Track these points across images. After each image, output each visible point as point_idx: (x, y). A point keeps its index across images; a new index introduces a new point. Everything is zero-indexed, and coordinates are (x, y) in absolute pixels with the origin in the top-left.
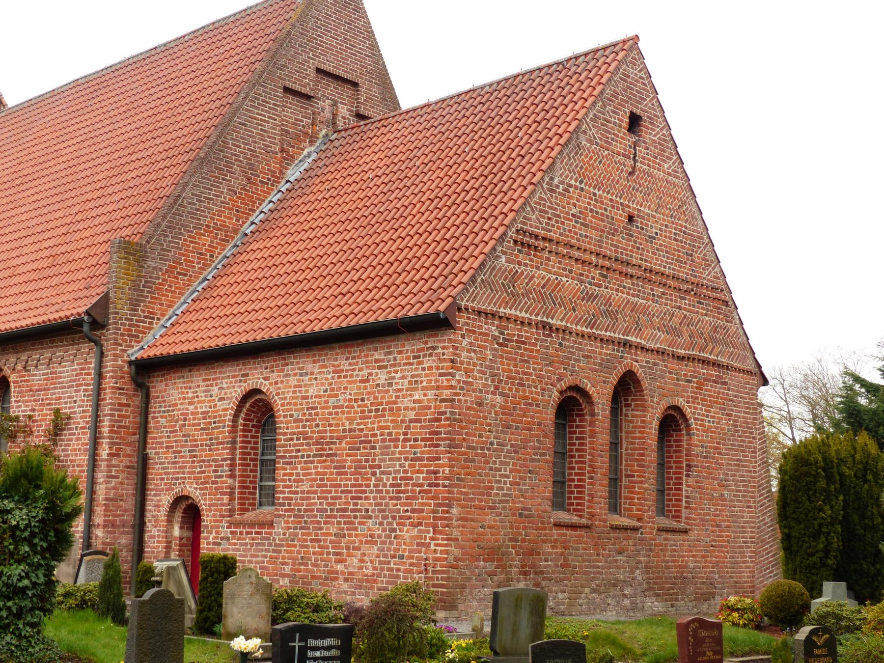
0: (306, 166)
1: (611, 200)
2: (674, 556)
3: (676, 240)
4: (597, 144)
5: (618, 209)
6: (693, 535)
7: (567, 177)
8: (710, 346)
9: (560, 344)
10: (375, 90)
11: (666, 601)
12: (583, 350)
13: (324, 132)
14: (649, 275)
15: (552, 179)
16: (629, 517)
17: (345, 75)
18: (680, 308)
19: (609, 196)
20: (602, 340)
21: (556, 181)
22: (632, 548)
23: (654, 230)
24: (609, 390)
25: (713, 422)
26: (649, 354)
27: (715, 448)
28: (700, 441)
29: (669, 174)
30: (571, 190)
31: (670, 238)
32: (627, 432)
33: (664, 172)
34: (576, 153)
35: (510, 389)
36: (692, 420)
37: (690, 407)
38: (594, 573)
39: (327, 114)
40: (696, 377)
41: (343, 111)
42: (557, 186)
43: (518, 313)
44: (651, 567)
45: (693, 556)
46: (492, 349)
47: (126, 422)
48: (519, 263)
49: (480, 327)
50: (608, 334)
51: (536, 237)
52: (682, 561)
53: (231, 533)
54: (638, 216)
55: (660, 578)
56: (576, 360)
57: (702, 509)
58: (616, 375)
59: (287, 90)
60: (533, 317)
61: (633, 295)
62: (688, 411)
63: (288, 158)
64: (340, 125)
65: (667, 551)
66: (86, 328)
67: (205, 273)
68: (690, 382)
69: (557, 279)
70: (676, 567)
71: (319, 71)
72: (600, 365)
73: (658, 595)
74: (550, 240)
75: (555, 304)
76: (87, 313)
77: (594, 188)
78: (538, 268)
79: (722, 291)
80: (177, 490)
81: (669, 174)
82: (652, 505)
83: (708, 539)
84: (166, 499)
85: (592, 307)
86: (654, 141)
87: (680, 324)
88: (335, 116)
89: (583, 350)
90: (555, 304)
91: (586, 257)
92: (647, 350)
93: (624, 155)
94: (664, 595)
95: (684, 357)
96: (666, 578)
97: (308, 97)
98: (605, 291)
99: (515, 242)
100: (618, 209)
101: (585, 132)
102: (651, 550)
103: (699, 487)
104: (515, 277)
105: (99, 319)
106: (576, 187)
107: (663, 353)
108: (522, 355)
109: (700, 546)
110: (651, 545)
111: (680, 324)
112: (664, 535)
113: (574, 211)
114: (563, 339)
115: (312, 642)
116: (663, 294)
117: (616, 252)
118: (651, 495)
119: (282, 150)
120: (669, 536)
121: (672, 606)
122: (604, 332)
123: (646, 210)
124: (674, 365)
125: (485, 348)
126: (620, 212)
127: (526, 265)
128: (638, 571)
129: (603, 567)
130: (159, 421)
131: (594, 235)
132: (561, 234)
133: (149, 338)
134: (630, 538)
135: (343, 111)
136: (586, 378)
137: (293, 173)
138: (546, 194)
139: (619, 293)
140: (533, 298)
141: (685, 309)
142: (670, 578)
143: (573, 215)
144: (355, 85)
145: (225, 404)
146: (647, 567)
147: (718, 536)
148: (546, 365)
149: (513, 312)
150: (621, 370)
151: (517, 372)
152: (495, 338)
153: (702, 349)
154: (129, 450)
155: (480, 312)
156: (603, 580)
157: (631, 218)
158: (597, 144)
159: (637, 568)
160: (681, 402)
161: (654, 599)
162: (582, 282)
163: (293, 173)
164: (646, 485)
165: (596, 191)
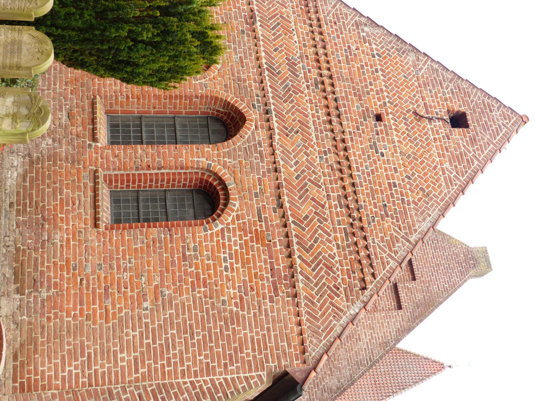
2: (68, 205)
3: (389, 184)
6: (92, 235)
7: (374, 39)
11: (18, 193)
14: (341, 146)
15: (366, 25)
19: (384, 88)
21: (366, 29)
22: (74, 131)
23: (384, 151)
25: (226, 268)
26: (268, 141)
28: (200, 242)
30: (367, 44)
36: (220, 226)
37: (233, 222)
38: (49, 79)
40: (267, 230)
44: (55, 164)
45: (68, 240)
50: (267, 78)
52: (62, 219)
54: (385, 125)
55: (43, 183)
56: (235, 49)
57: (124, 258)
58: (236, 102)
61: (314, 122)
65: (73, 192)
69: (293, 30)
70: (55, 207)
72: (240, 80)
73: (24, 180)
75: (273, 29)
79: (373, 275)
82: (120, 160)
83: (89, 270)
85: (285, 69)
87: (313, 199)
90: (273, 29)
92: (271, 145)
93: (425, 104)
94: (25, 187)
95: (281, 206)
96: (44, 189)
98: (304, 85)
102: (73, 162)
107: (276, 170)
109: (81, 255)
110: (79, 164)
111: (313, 199)
112: (90, 184)
113: (353, 48)
118: (130, 159)
120: (90, 193)
121: (11, 205)
122: (269, 84)
123: (396, 139)
124: (270, 191)
126: (379, 103)
128: (50, 142)
129: (55, 89)
131: (345, 71)
134: (84, 129)
136: (224, 62)
138: (352, 19)
139: (309, 101)
140: (270, 8)
141: (330, 207)
142: (43, 200)
143: (349, 47)
146: (55, 154)
147: (94, 292)
148: (222, 18)
156: (43, 90)
157: (379, 118)
159: (54, 140)
160: (235, 204)
161: (20, 170)
162: (301, 57)
164: (140, 151)
165: (380, 73)
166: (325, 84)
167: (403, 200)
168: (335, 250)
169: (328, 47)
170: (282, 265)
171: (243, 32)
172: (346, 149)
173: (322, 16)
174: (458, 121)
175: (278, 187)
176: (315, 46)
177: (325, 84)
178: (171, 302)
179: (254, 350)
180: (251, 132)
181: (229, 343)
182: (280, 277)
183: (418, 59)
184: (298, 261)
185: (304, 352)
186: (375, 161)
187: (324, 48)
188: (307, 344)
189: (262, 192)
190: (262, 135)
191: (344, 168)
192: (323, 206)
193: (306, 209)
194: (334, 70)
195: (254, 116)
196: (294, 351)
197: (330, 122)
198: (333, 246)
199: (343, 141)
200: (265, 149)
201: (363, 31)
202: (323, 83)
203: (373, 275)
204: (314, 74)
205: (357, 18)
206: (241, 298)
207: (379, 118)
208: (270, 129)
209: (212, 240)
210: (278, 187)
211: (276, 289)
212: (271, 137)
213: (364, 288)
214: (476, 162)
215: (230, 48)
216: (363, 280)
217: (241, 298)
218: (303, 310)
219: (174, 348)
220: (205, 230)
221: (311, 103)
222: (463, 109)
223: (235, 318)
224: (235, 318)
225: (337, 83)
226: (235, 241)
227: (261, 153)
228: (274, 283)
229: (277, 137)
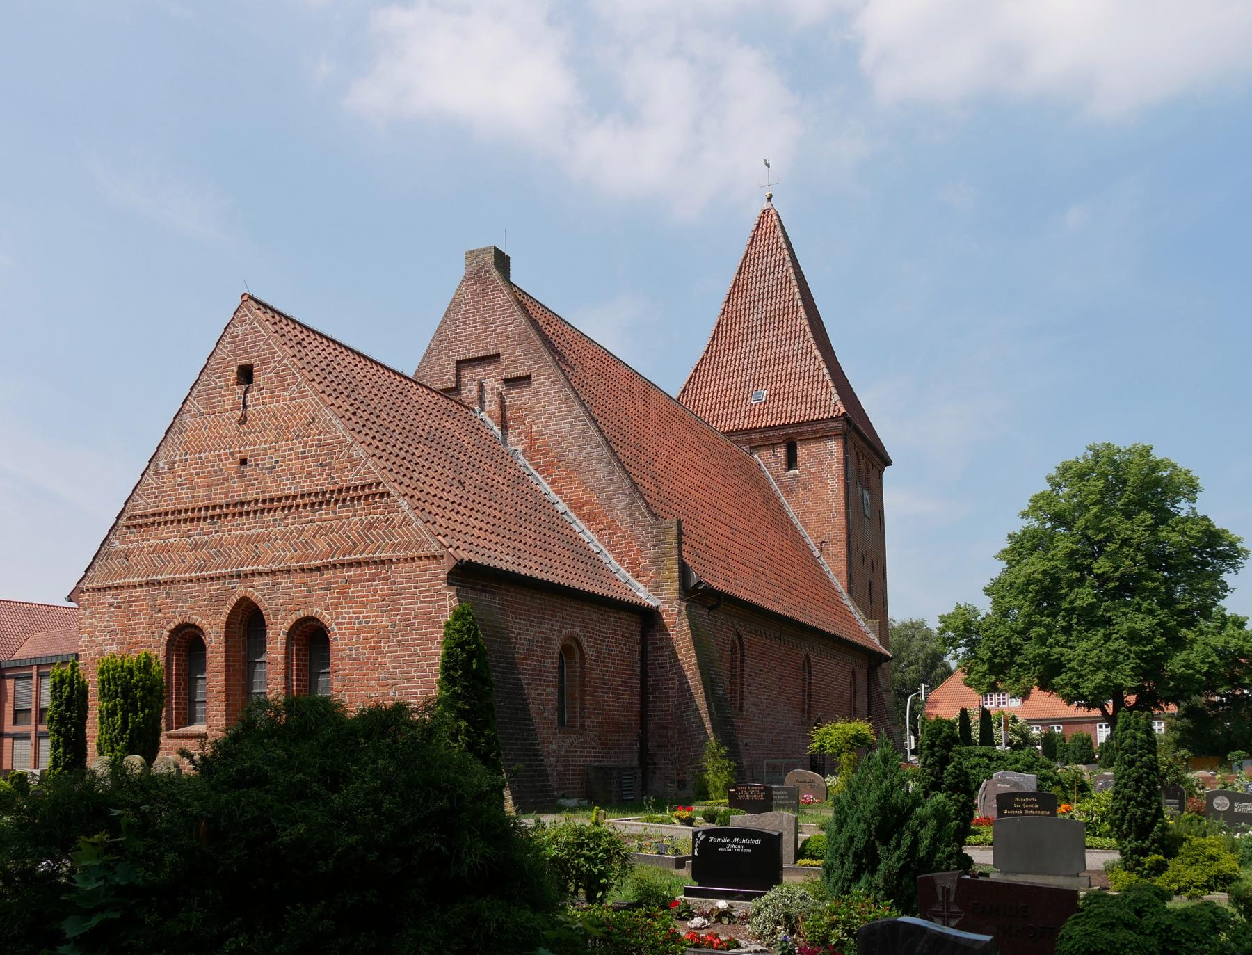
5: (227, 459)
14: (268, 504)
21: (161, 465)
24: (223, 618)
25: (367, 622)
27: (374, 648)
37: (330, 614)
48: (131, 542)
74: (160, 514)
79: (379, 484)
81: (294, 399)
85: (202, 554)
92: (267, 574)
95: (318, 569)
99: (128, 527)
101: (189, 411)
103: (347, 690)
107: (288, 571)
117: (226, 497)
123: (263, 446)
124: (306, 578)
131: (201, 492)
141: (320, 520)
155: (99, 590)
157: (244, 462)
158: (202, 414)
160: (314, 611)
166: (216, 513)
167: (318, 446)
168: (357, 519)
169: (179, 507)
170: (366, 571)
171: (167, 594)
172: (272, 500)
173: (150, 511)
174: (246, 375)
175: (303, 570)
176: (179, 521)
177: (216, 513)
178: (390, 673)
179: (430, 602)
180: (255, 590)
181: (424, 623)
182: (376, 574)
183: (189, 411)
184: (364, 555)
185: (435, 557)
186: (283, 471)
187: (180, 512)
188: (428, 553)
189: (306, 585)
190: (258, 581)
191: (287, 503)
192: (321, 528)
193: (322, 544)
194: (200, 504)
195: (242, 589)
196: (433, 565)
197: (248, 513)
198: (353, 518)
199: (264, 502)
200: (270, 580)
202: (212, 517)
203: (379, 484)
204: (205, 525)
206: (391, 610)
207: (244, 462)
208: (253, 574)
209: (344, 634)
210: (303, 570)
211: (384, 578)
212: (260, 574)
213: (388, 494)
214: (285, 361)
216: (382, 495)
217: (391, 610)
218: (402, 554)
219: (424, 671)
220: (336, 639)
221: (230, 530)
222: (235, 368)
223: (405, 617)
224: (405, 617)
225: (212, 502)
226: (345, 612)
227: (274, 584)
228: (380, 580)
229: (260, 567)
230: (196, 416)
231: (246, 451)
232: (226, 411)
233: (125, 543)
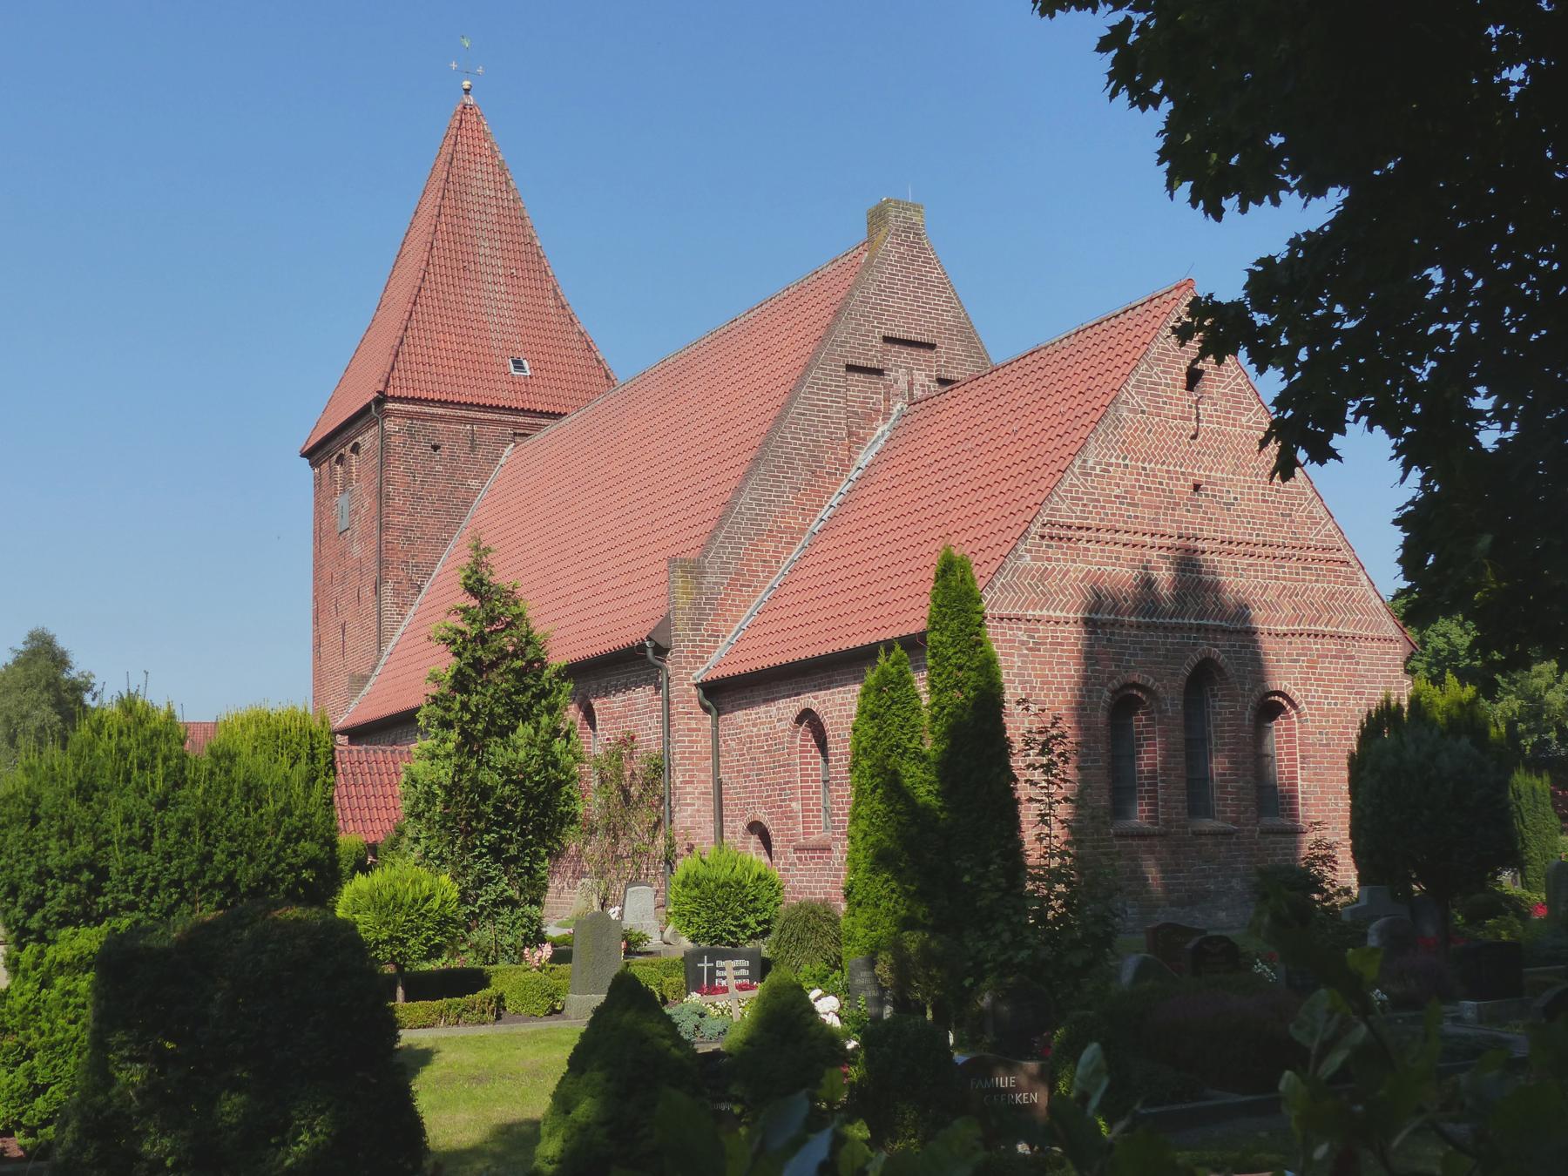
0: (877, 448)
1: (1168, 472)
4: (1143, 412)
5: (1178, 479)
8: (1326, 616)
9: (1109, 640)
10: (958, 348)
12: (1140, 643)
13: (898, 407)
15: (1085, 461)
16: (1224, 820)
17: (919, 338)
18: (1277, 578)
20: (1165, 628)
21: (1090, 463)
24: (1181, 681)
26: (1234, 637)
27: (1341, 734)
29: (1250, 428)
31: (1257, 501)
32: (1216, 726)
33: (1241, 426)
34: (1116, 427)
35: (1047, 696)
39: (903, 385)
41: (920, 377)
42: (1093, 468)
43: (1051, 613)
46: (1020, 656)
47: (698, 747)
48: (1049, 559)
49: (1004, 634)
51: (1069, 527)
53: (799, 859)
59: (851, 368)
60: (1071, 615)
62: (1296, 696)
63: (856, 439)
64: (918, 393)
66: (650, 653)
67: (772, 581)
68: (1297, 661)
71: (887, 339)
72: (1166, 656)
76: (649, 638)
77: (1144, 460)
78: (1074, 561)
80: (749, 817)
81: (1250, 428)
84: (742, 825)
86: (1224, 394)
88: (911, 385)
89: (1140, 643)
91: (1138, 538)
92: (1231, 633)
97: (879, 372)
99: (1043, 537)
100: (1178, 479)
104: (1045, 575)
105: (663, 643)
106: (1118, 465)
108: (1060, 657)
112: (1272, 838)
113: (1117, 492)
114: (1112, 634)
115: (720, 964)
116: (1250, 565)
117: (1179, 528)
119: (850, 434)
123: (1219, 474)
125: (1012, 655)
127: (1058, 560)
130: (730, 744)
132: (1102, 520)
133: (713, 659)
135: (920, 377)
137: (864, 458)
144: (932, 346)
145: (780, 726)
149: (1045, 612)
150: (1195, 659)
151: (1055, 676)
152: (1023, 643)
153: (1315, 621)
154: (702, 776)
157: (1197, 487)
158: (1143, 412)
163: (864, 458)
170: (1332, 646)
201: (1093, 468)
205: (1076, 471)
212: (1224, 631)
215: (1128, 661)
227: (1242, 647)
230: (1134, 411)
231: (1200, 475)
232: (1174, 418)
233: (1041, 559)
